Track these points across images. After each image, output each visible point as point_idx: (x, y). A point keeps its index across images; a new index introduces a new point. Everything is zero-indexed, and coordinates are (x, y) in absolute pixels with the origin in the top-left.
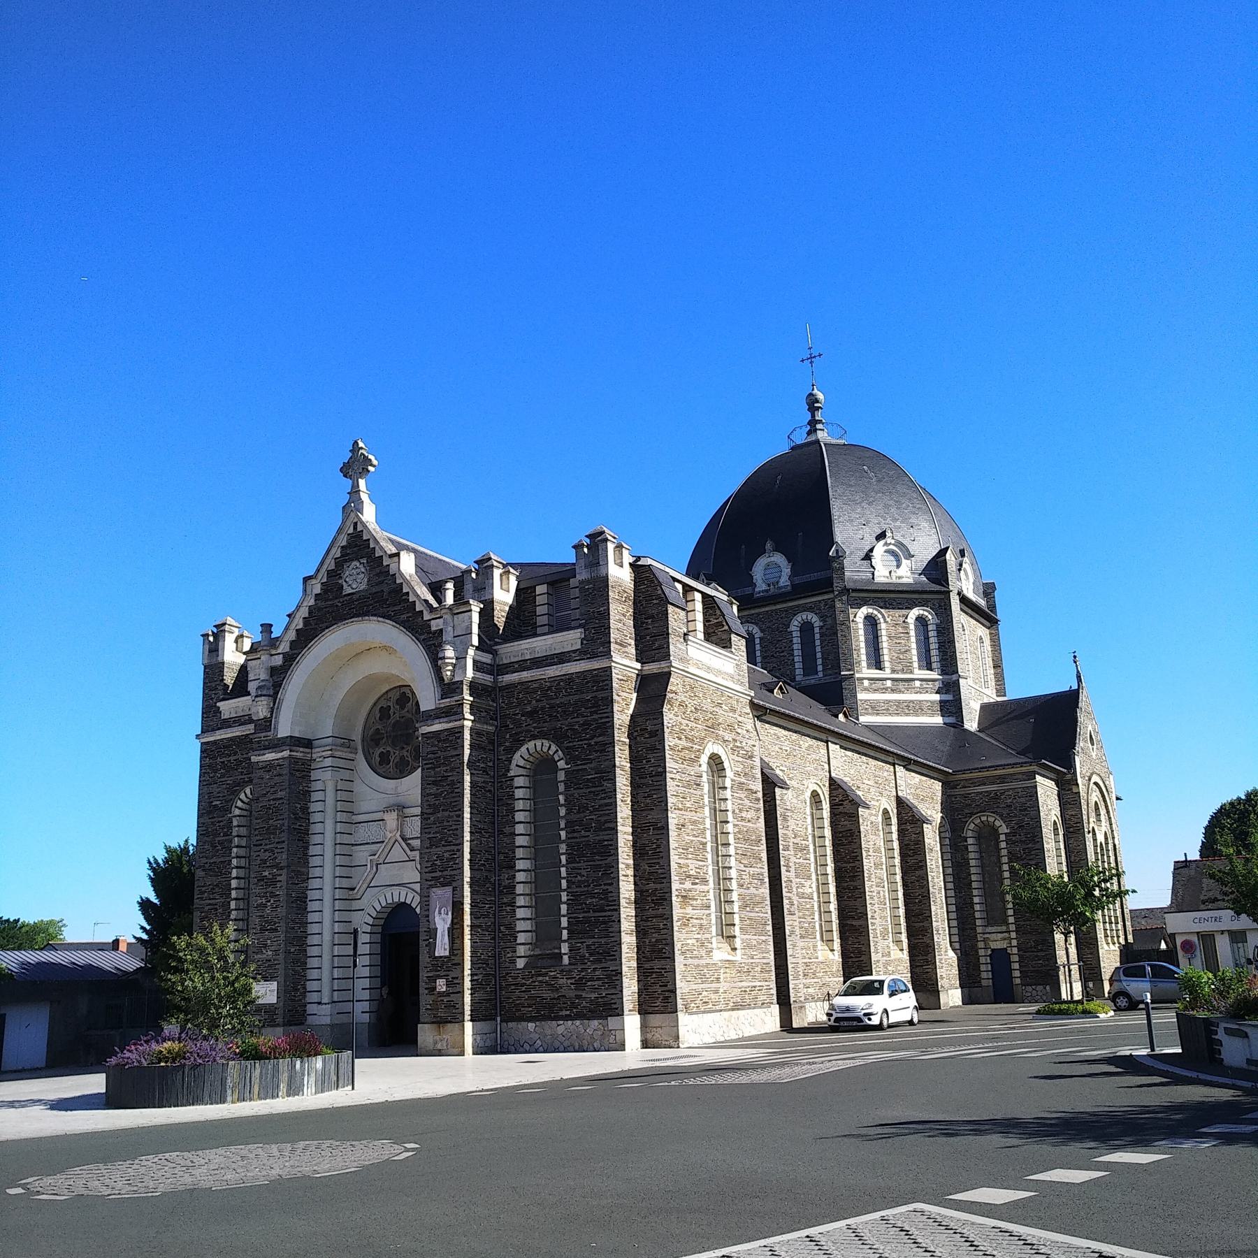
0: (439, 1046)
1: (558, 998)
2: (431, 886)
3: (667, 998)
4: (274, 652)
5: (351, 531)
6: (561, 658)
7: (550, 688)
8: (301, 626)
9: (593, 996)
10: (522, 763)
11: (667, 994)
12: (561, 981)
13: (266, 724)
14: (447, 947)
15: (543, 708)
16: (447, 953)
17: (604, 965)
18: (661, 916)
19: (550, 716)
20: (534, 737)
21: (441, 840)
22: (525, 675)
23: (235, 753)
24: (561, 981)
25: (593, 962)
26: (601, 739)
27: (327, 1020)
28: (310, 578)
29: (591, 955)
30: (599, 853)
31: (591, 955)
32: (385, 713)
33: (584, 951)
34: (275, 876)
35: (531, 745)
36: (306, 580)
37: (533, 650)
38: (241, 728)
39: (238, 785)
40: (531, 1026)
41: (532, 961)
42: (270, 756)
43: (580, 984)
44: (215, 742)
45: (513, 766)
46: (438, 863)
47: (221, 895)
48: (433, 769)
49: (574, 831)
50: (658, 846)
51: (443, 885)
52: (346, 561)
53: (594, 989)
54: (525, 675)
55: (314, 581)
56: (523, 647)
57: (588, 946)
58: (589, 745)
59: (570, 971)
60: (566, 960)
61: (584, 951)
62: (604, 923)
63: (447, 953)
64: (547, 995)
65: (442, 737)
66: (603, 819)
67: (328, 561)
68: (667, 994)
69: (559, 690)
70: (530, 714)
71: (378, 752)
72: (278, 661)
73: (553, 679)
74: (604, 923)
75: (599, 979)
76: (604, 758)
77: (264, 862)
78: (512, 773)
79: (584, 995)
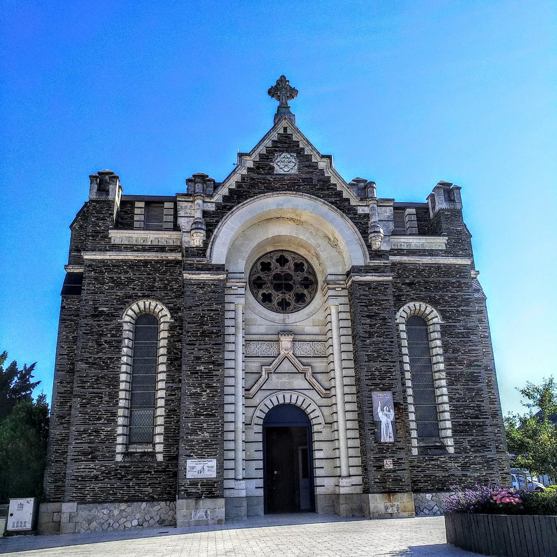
0: (390, 511)
1: (449, 476)
2: (371, 390)
3: (504, 478)
4: (207, 200)
5: (281, 131)
6: (431, 253)
7: (423, 270)
8: (234, 187)
9: (476, 475)
10: (432, 315)
11: (504, 475)
12: (450, 465)
13: (202, 251)
14: (392, 435)
15: (419, 282)
16: (392, 440)
17: (481, 454)
18: (496, 425)
19: (426, 288)
20: (413, 300)
21: (378, 357)
22: (405, 259)
23: (127, 272)
24: (450, 465)
25: (475, 452)
26: (465, 308)
27: (243, 494)
28: (246, 155)
29: (472, 447)
30: (472, 381)
31: (472, 447)
32: (266, 267)
33: (466, 444)
34: (210, 371)
35: (411, 304)
36: (241, 155)
37: (409, 244)
38: (136, 254)
39: (130, 297)
40: (428, 496)
41: (423, 450)
42: (204, 276)
43: (464, 467)
44: (103, 261)
45: (397, 316)
46: (377, 373)
47: (108, 386)
48: (367, 306)
49: (450, 365)
50: (490, 381)
51: (383, 390)
52: (276, 151)
53: (476, 470)
54: (405, 259)
55: (248, 158)
56: (402, 240)
57: (469, 441)
58: (458, 311)
59: (456, 458)
60: (451, 450)
61: (466, 444)
62: (479, 426)
63: (392, 440)
64: (440, 474)
65: (373, 286)
66: (473, 358)
67: (261, 148)
68: (504, 475)
69: (430, 273)
70: (410, 284)
71: (260, 293)
72: (211, 208)
73: (426, 265)
74: (479, 426)
75: (479, 464)
76: (469, 320)
77: (198, 358)
78: (398, 321)
79: (469, 474)
